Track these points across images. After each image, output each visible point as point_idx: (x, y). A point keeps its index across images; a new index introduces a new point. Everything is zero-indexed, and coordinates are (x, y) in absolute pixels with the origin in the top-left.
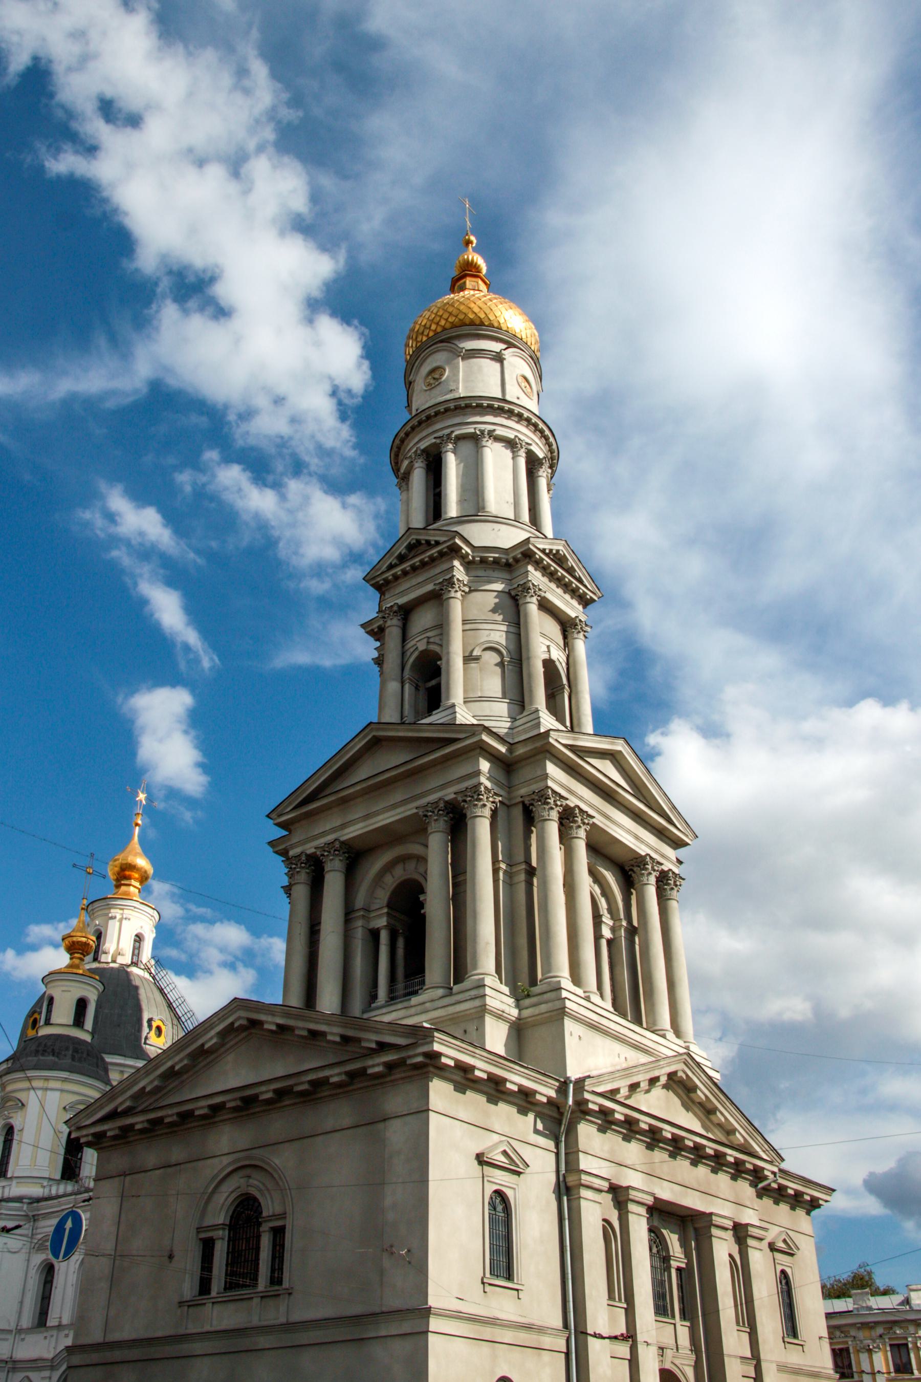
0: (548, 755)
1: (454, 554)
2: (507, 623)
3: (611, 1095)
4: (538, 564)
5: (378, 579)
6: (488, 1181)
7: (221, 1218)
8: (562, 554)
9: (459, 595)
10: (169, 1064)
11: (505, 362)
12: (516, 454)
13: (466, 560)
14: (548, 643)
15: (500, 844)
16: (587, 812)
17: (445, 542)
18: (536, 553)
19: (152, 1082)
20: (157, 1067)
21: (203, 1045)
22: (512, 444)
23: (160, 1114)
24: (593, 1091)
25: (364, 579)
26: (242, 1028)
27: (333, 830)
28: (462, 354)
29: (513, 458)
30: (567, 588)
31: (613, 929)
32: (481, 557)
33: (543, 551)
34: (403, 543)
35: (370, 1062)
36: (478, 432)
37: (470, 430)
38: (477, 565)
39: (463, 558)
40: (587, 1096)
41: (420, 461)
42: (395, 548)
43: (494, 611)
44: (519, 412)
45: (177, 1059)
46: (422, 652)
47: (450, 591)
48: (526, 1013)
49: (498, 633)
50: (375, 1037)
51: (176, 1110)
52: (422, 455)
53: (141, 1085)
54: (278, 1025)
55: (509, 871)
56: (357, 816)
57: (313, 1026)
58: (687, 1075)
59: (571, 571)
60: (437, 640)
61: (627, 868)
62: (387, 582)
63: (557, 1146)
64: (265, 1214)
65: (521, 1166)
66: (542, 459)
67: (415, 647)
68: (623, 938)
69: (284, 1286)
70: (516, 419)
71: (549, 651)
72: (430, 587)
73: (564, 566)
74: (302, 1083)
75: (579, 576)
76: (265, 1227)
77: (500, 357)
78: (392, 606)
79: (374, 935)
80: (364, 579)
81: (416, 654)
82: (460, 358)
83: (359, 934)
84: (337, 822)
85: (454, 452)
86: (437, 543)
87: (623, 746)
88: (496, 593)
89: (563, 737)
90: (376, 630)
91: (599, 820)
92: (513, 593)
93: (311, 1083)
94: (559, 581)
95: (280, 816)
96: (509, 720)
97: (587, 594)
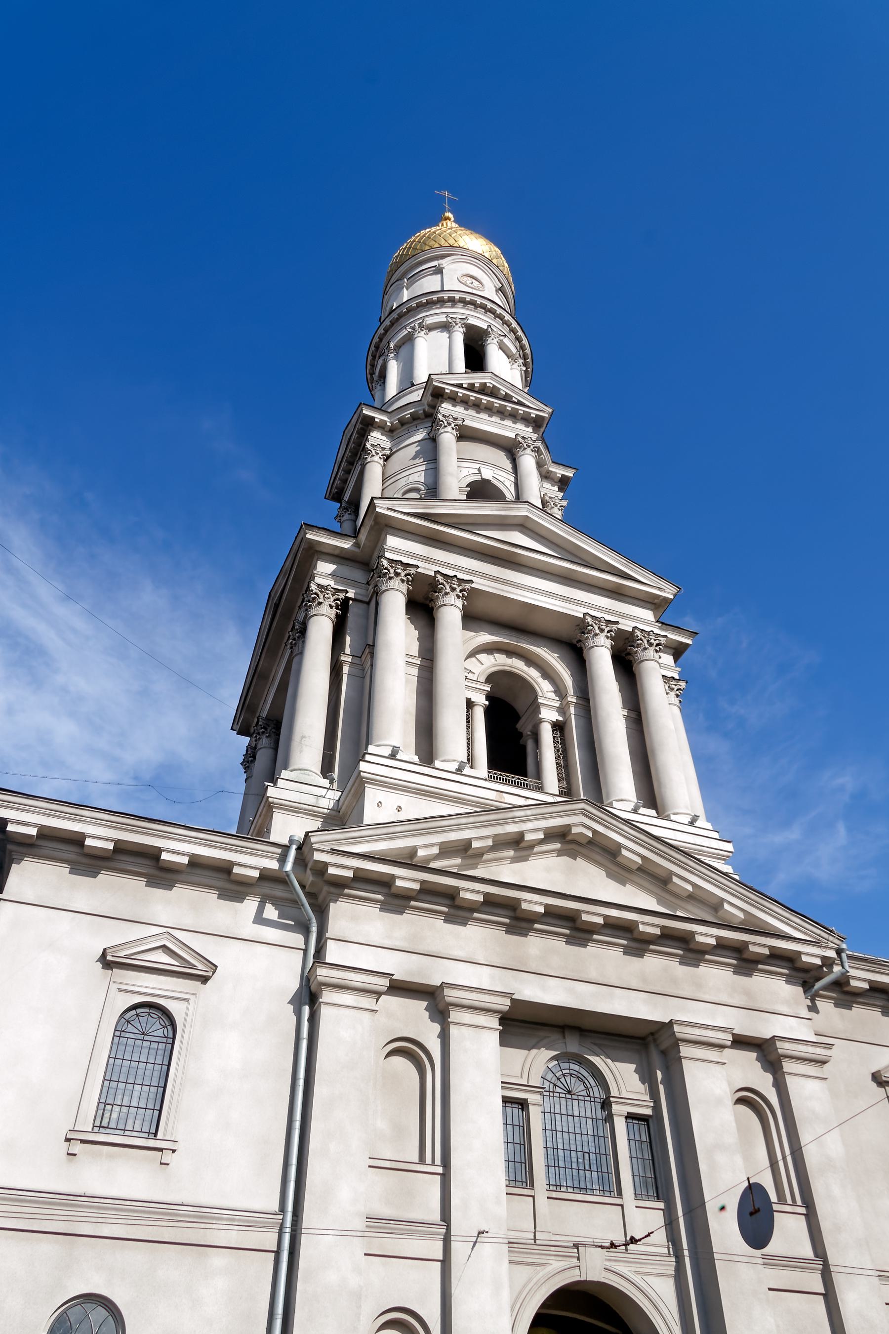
0: (389, 530)
1: (370, 427)
2: (426, 463)
3: (408, 860)
4: (453, 399)
6: (120, 990)
8: (491, 386)
9: (376, 458)
12: (450, 331)
13: (387, 429)
14: (477, 466)
15: (348, 639)
16: (455, 576)
18: (444, 389)
24: (331, 849)
25: (325, 498)
28: (405, 284)
29: (449, 337)
30: (502, 413)
31: (562, 710)
32: (398, 419)
33: (460, 386)
37: (405, 332)
38: (400, 429)
39: (381, 427)
40: (318, 856)
43: (414, 458)
44: (448, 297)
52: (381, 380)
55: (358, 662)
58: (595, 832)
59: (507, 398)
61: (574, 642)
63: (307, 943)
65: (200, 966)
66: (488, 329)
68: (573, 716)
70: (449, 304)
71: (480, 472)
73: (499, 397)
75: (518, 400)
77: (439, 270)
80: (325, 498)
82: (405, 288)
85: (396, 357)
87: (528, 511)
88: (418, 443)
89: (405, 506)
91: (479, 584)
92: (431, 436)
94: (489, 410)
97: (530, 413)
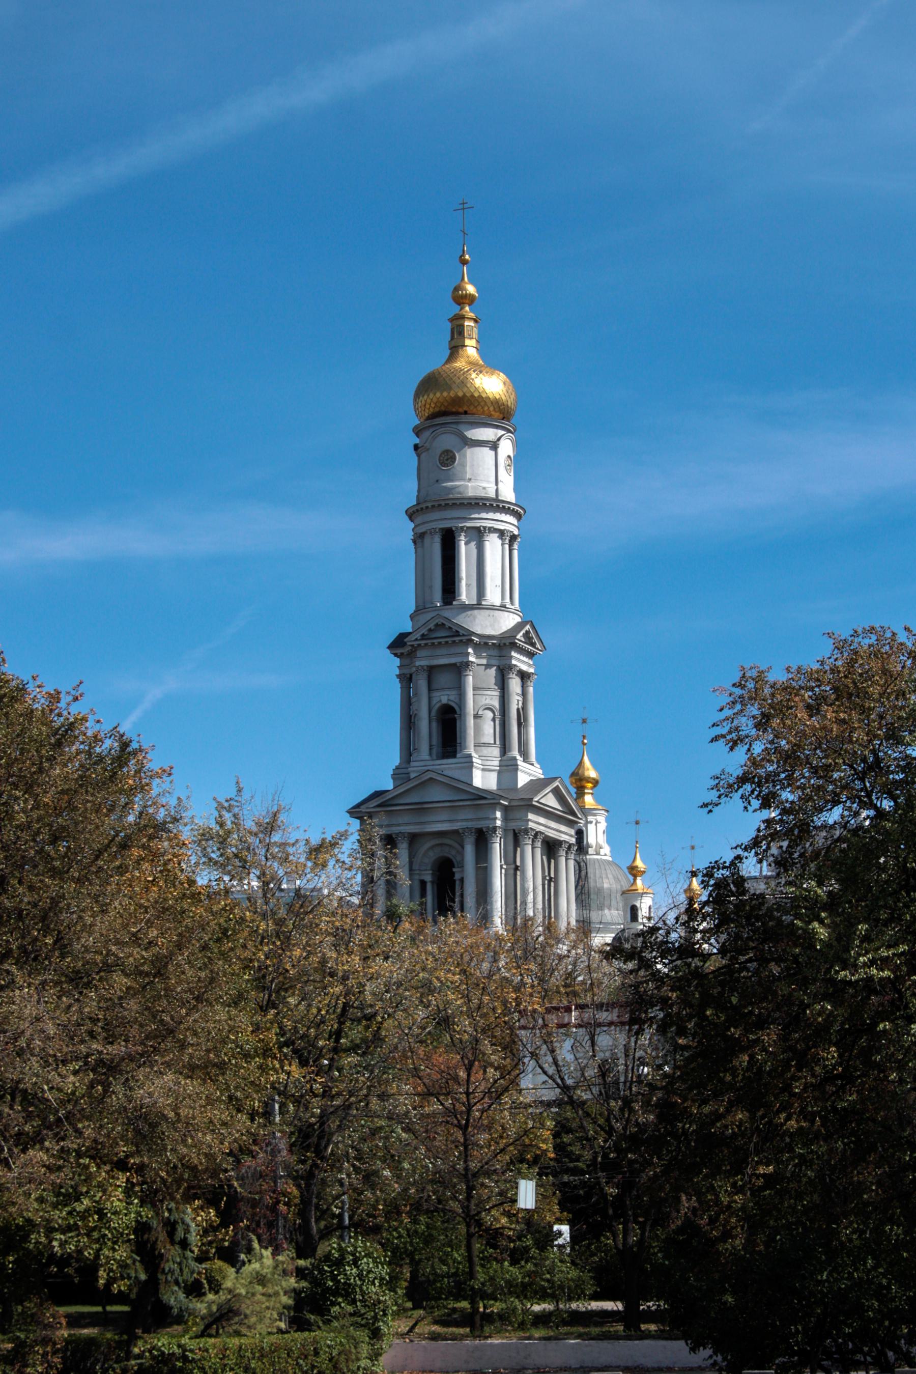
17: (464, 635)
22: (501, 533)
67: (438, 699)
72: (452, 660)
79: (423, 883)
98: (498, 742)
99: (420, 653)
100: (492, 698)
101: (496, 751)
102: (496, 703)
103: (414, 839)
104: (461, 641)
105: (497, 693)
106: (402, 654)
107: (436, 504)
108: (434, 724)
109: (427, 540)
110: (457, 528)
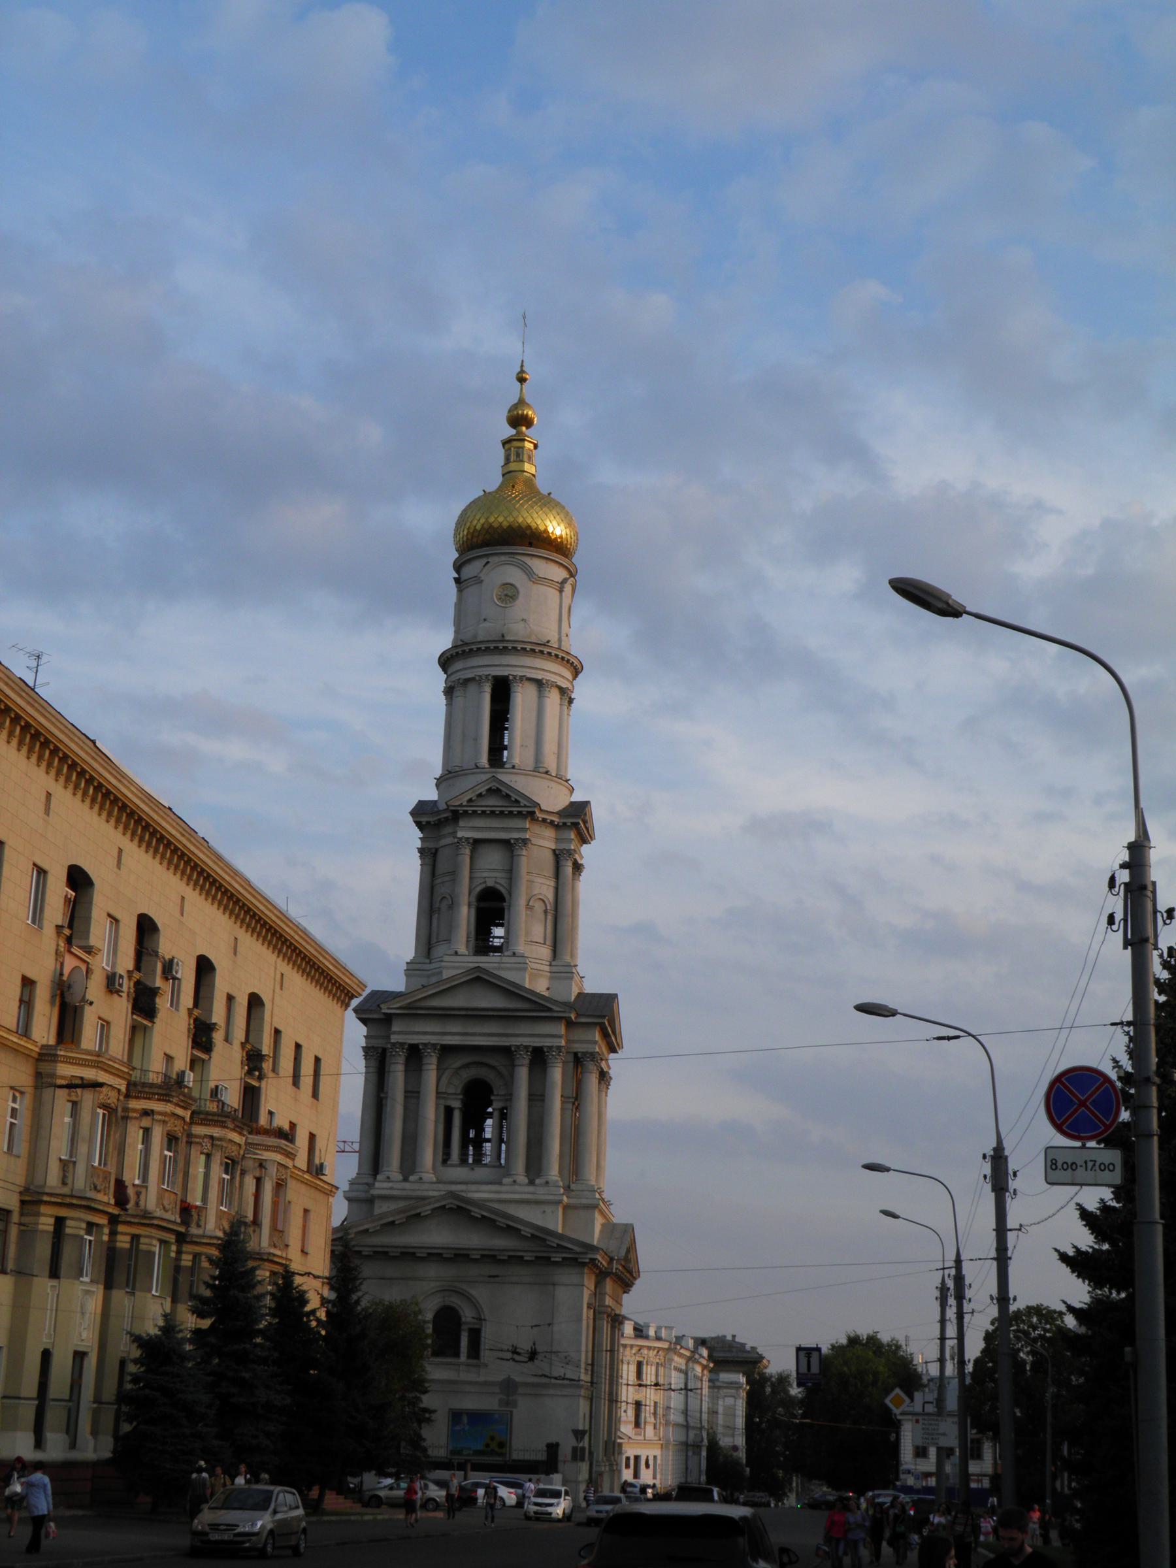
5: (459, 808)
7: (429, 1316)
10: (391, 1219)
11: (563, 594)
17: (525, 806)
19: (375, 1227)
20: (381, 1219)
21: (419, 1214)
23: (386, 1250)
26: (451, 1209)
27: (433, 1033)
29: (561, 705)
34: (484, 786)
35: (554, 1255)
36: (544, 681)
41: (487, 684)
42: (477, 788)
45: (397, 1217)
46: (491, 888)
47: (522, 849)
48: (572, 1201)
49: (545, 887)
50: (557, 1241)
51: (399, 1250)
53: (366, 1227)
54: (482, 1216)
56: (454, 1030)
57: (511, 1223)
60: (503, 882)
62: (466, 812)
64: (463, 1319)
67: (483, 880)
69: (482, 1361)
74: (504, 1255)
76: (464, 1327)
78: (468, 838)
79: (449, 1111)
81: (483, 886)
83: (442, 1109)
84: (438, 1029)
86: (517, 801)
90: (424, 823)
92: (557, 852)
93: (509, 1256)
95: (389, 1008)
96: (548, 963)
98: (549, 942)
99: (462, 823)
100: (545, 888)
101: (545, 952)
102: (550, 895)
103: (446, 1051)
104: (520, 813)
105: (552, 883)
106: (428, 823)
107: (492, 646)
108: (473, 912)
109: (472, 688)
110: (515, 677)
